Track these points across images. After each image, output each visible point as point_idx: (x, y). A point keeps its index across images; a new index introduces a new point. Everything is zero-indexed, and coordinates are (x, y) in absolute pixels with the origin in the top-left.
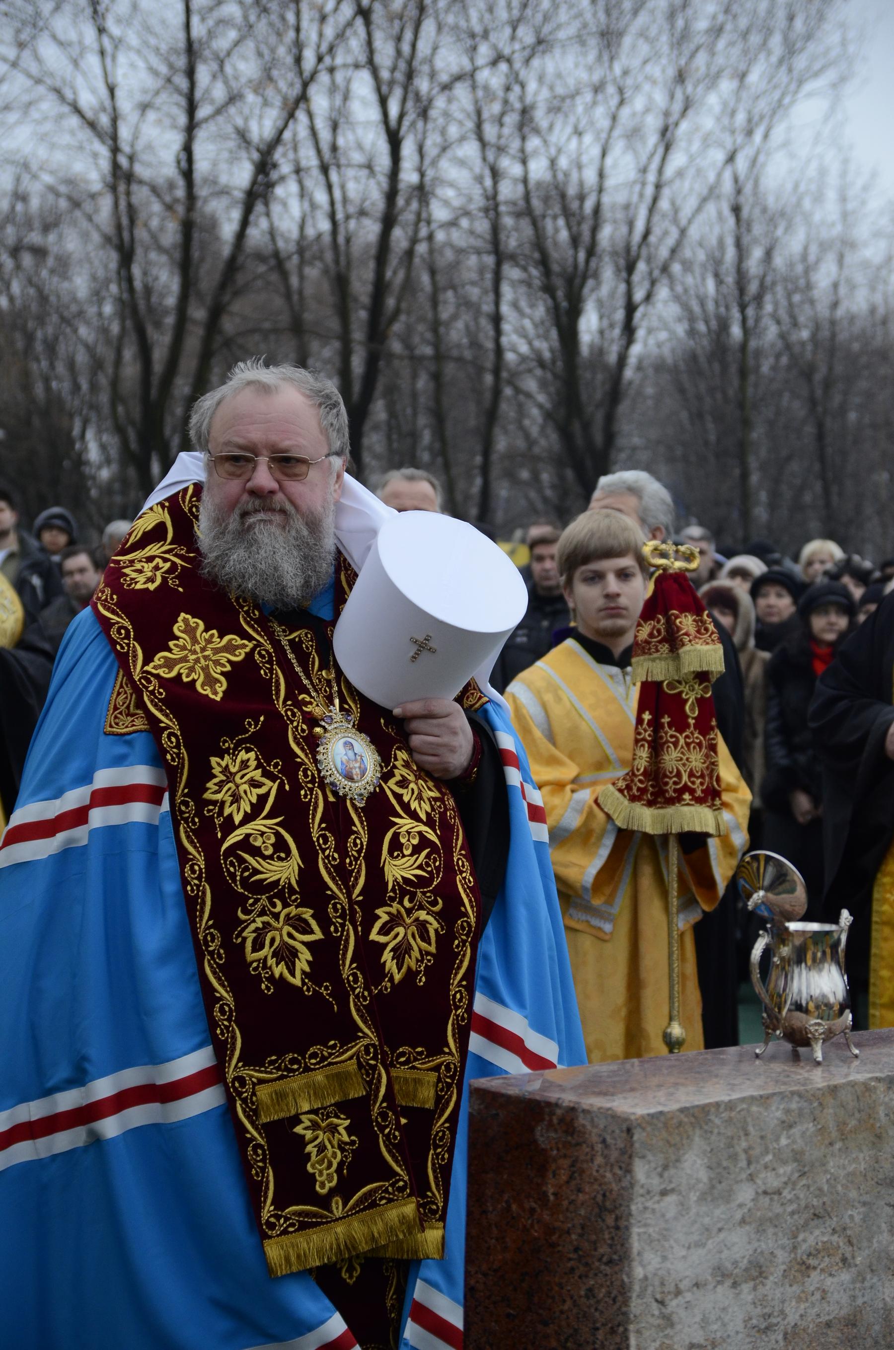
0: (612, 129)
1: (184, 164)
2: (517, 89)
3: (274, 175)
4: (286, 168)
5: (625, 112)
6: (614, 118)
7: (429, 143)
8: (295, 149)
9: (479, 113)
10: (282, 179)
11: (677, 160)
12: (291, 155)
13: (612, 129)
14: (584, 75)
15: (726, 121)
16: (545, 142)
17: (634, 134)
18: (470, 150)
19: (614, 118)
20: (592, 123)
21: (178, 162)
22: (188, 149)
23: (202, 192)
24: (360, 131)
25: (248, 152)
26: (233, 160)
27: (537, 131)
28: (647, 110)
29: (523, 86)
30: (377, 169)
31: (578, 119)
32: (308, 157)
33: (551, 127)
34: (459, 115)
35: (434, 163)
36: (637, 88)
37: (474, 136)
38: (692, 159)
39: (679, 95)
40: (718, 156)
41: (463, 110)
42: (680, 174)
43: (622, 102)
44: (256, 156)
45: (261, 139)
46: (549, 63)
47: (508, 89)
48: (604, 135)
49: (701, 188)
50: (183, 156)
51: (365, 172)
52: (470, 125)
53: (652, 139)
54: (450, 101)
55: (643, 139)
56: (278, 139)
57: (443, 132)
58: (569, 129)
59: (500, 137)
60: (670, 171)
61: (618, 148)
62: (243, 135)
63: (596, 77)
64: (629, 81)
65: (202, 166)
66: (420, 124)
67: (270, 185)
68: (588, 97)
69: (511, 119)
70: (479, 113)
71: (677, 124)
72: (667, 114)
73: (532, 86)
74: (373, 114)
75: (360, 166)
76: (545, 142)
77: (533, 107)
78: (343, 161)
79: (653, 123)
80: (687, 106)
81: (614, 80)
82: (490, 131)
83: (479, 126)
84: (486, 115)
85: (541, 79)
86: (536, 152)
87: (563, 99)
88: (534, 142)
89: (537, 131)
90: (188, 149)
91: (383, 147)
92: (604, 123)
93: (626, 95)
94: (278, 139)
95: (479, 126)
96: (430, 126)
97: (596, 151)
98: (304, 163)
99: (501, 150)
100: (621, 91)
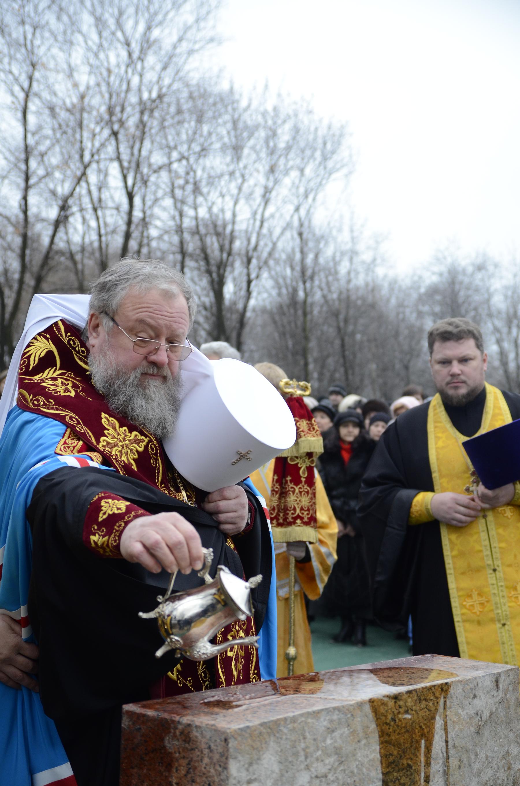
0: (239, 194)
1: (23, 207)
2: (192, 174)
3: (68, 213)
4: (75, 209)
5: (246, 185)
6: (240, 189)
7: (147, 198)
8: (80, 199)
9: (173, 184)
10: (73, 214)
11: (271, 209)
12: (77, 202)
13: (239, 194)
14: (224, 168)
15: (294, 190)
16: (206, 200)
17: (250, 196)
18: (168, 202)
19: (240, 189)
20: (229, 191)
21: (20, 206)
22: (25, 198)
23: (31, 219)
24: (112, 191)
25: (56, 200)
26: (50, 205)
27: (201, 194)
28: (256, 185)
29: (195, 172)
30: (121, 209)
31: (222, 188)
32: (86, 202)
33: (209, 193)
34: (163, 186)
35: (151, 207)
36: (251, 175)
37: (170, 195)
38: (278, 209)
39: (272, 178)
40: (291, 208)
41: (164, 183)
42: (272, 216)
43: (244, 180)
44: (60, 203)
45: (63, 195)
46: (208, 162)
47: (188, 173)
48: (235, 197)
49: (282, 224)
50: (23, 203)
51: (115, 212)
52: (168, 190)
53: (258, 199)
54: (158, 178)
55: (254, 200)
56: (71, 194)
57: (155, 193)
58: (217, 194)
59: (183, 195)
60: (267, 214)
61: (242, 202)
62: (54, 193)
63: (231, 168)
64: (247, 171)
65: (32, 210)
66: (143, 190)
67: (66, 217)
68: (227, 177)
69: (190, 188)
70: (173, 184)
71: (270, 192)
72: (266, 188)
73: (199, 173)
74: (120, 184)
75: (112, 208)
76: (206, 200)
77: (200, 181)
78: (103, 205)
79: (259, 192)
80: (276, 182)
81: (239, 170)
82: (178, 193)
83: (172, 191)
84: (176, 185)
85: (204, 169)
86: (201, 205)
87: (214, 178)
88: (200, 199)
89: (201, 194)
90: (25, 198)
91: (125, 201)
92: (235, 191)
93: (246, 178)
94: (71, 194)
95: (172, 191)
96: (148, 190)
97: (231, 204)
98: (84, 206)
99: (183, 202)
100: (243, 176)
